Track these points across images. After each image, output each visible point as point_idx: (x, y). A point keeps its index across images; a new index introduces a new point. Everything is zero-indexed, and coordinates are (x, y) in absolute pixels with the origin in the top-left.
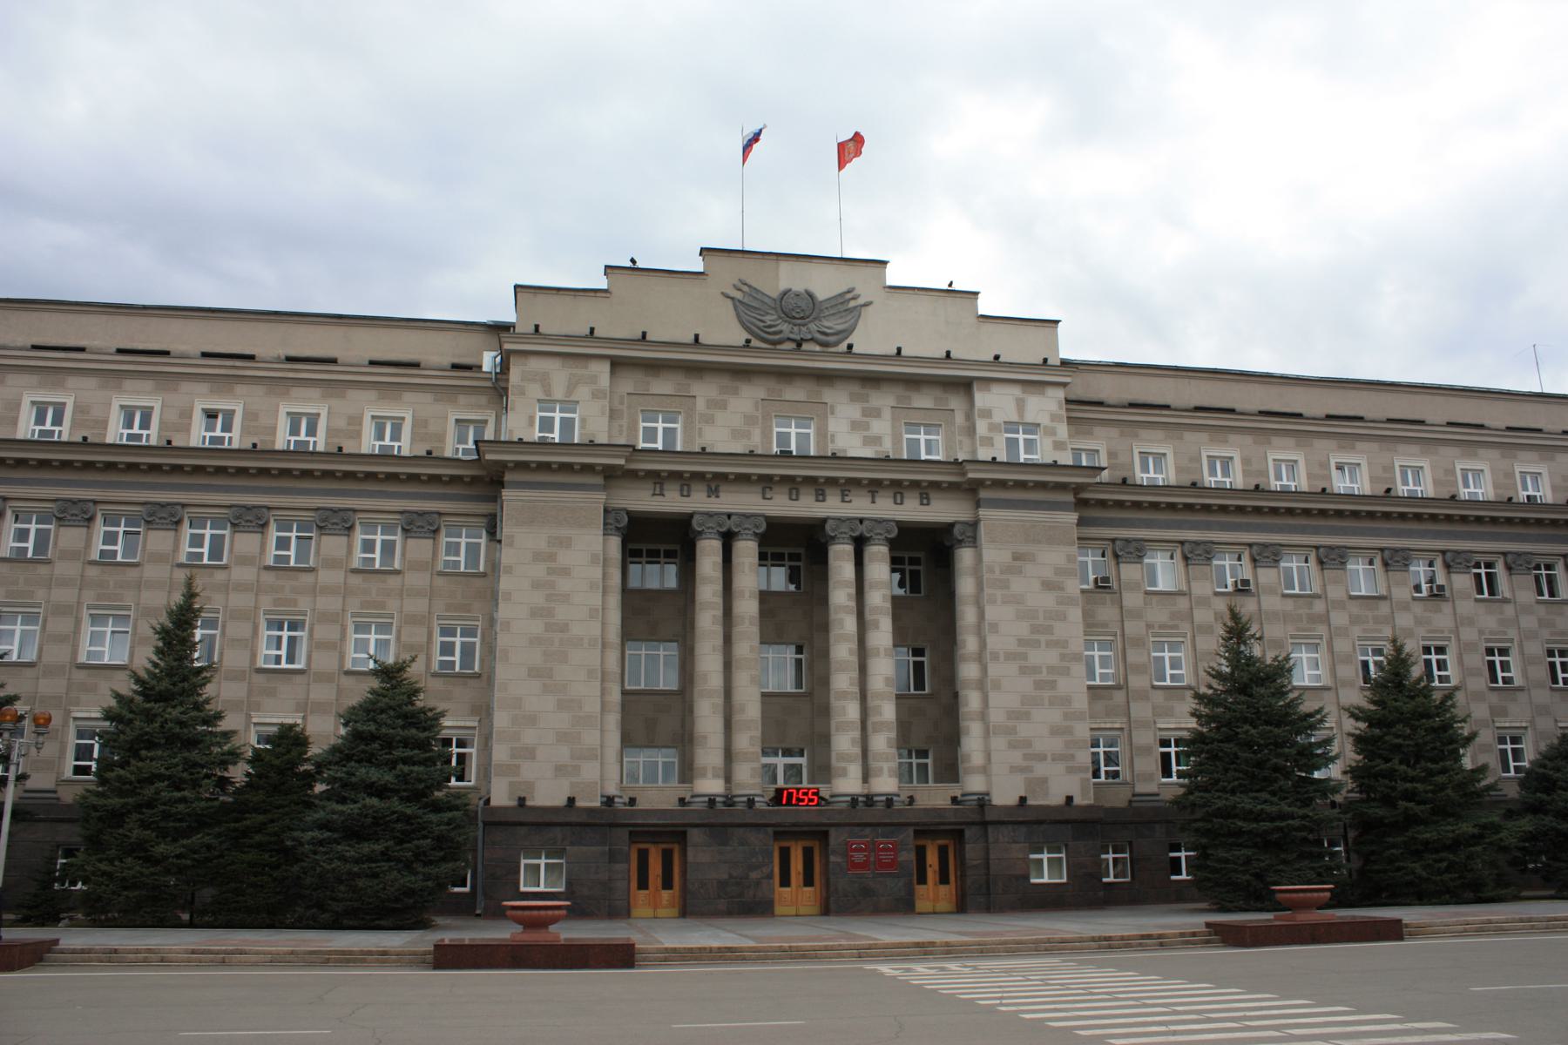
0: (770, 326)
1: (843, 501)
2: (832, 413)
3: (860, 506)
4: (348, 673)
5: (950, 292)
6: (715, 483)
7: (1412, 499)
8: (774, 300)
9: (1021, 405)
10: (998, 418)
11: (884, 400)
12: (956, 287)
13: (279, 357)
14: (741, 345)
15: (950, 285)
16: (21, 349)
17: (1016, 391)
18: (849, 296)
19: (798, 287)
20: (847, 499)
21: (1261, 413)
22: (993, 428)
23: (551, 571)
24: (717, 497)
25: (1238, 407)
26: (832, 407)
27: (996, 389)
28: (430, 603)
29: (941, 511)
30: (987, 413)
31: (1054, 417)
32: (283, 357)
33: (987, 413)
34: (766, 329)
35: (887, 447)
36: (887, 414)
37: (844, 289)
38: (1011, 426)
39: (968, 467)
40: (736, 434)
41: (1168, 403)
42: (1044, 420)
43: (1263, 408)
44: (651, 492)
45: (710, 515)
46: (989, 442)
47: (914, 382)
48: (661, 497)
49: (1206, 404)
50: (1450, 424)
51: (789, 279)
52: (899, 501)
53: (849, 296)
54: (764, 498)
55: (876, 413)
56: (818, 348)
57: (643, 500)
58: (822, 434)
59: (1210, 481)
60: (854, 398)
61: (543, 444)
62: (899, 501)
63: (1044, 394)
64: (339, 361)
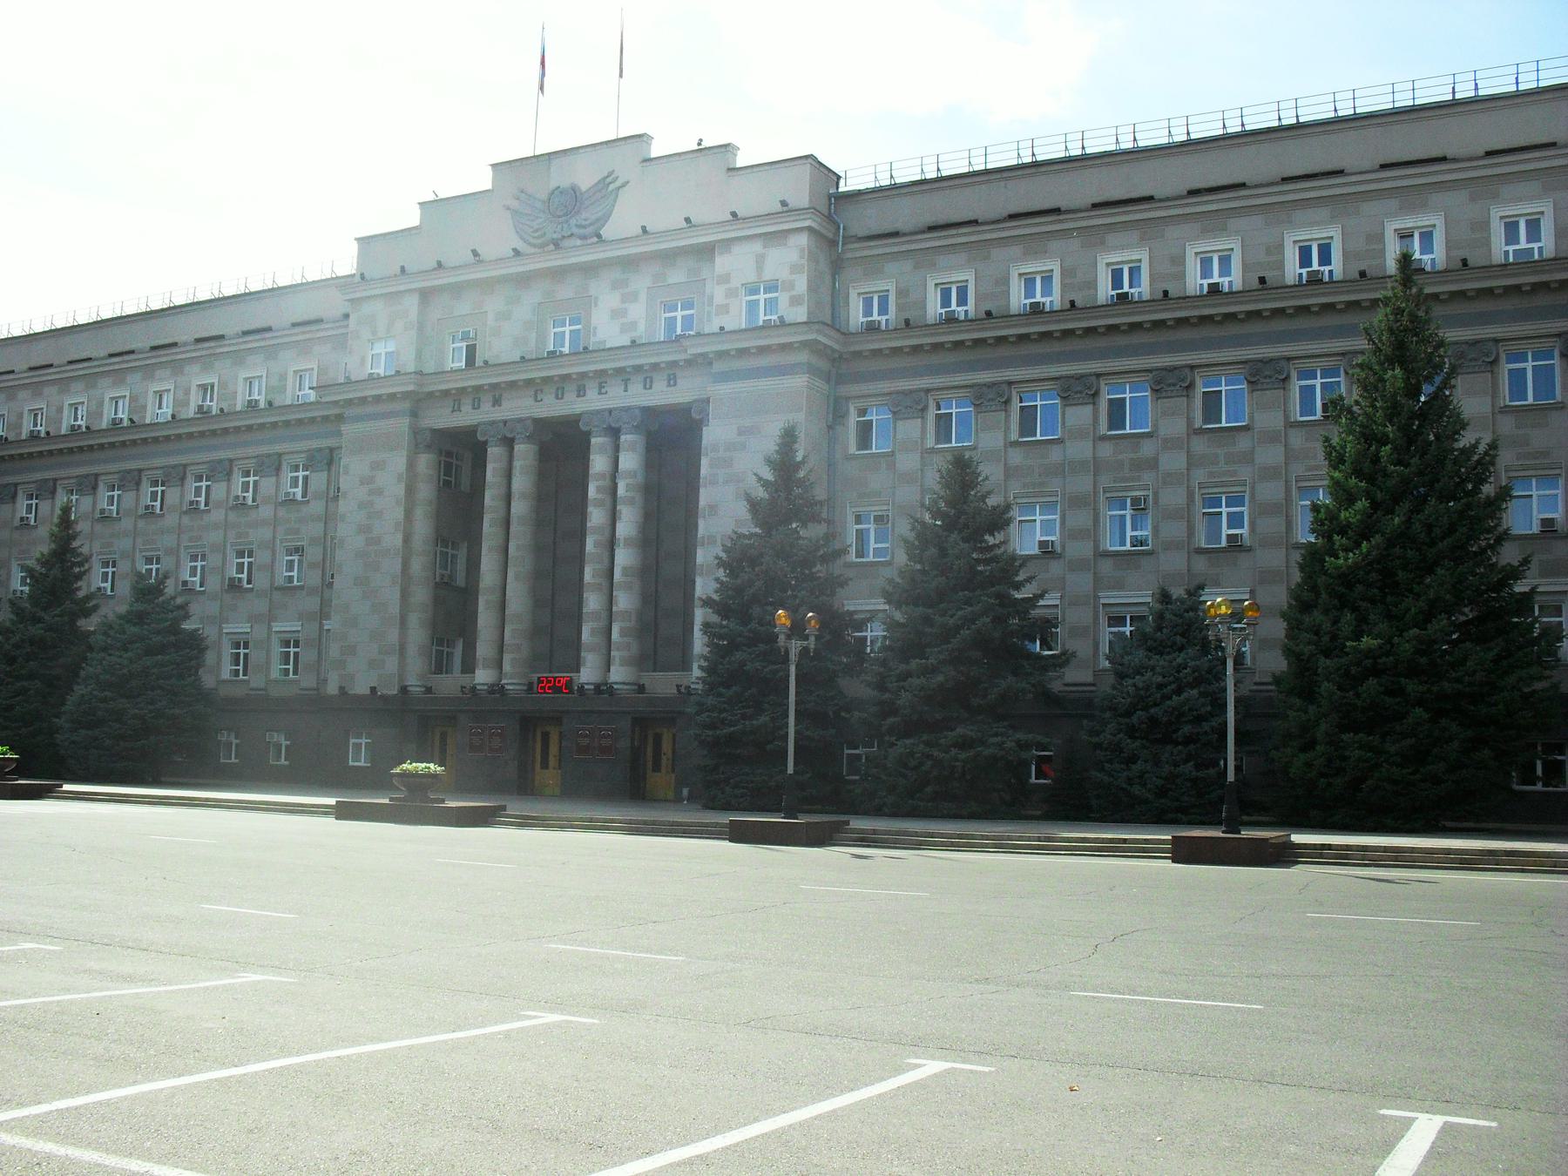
0: (537, 231)
1: (600, 393)
2: (596, 305)
3: (618, 397)
5: (701, 151)
7: (1525, 263)
8: (544, 202)
9: (760, 260)
10: (736, 282)
11: (641, 282)
12: (705, 144)
13: (238, 334)
14: (511, 256)
15: (699, 144)
16: (102, 359)
17: (757, 247)
18: (609, 180)
19: (565, 183)
20: (603, 391)
22: (732, 293)
23: (371, 492)
24: (500, 406)
25: (1063, 205)
26: (596, 298)
27: (737, 249)
28: (325, 527)
31: (795, 269)
32: (240, 333)
33: (725, 279)
34: (533, 234)
35: (641, 333)
36: (643, 297)
41: (1240, 180)
42: (784, 274)
44: (451, 409)
45: (493, 423)
46: (724, 309)
47: (669, 257)
48: (458, 413)
50: (1384, 167)
51: (559, 177)
52: (648, 386)
53: (609, 180)
54: (536, 401)
55: (631, 297)
56: (579, 242)
57: (443, 418)
59: (1507, 253)
60: (615, 285)
61: (372, 378)
62: (648, 386)
63: (785, 245)
64: (273, 329)
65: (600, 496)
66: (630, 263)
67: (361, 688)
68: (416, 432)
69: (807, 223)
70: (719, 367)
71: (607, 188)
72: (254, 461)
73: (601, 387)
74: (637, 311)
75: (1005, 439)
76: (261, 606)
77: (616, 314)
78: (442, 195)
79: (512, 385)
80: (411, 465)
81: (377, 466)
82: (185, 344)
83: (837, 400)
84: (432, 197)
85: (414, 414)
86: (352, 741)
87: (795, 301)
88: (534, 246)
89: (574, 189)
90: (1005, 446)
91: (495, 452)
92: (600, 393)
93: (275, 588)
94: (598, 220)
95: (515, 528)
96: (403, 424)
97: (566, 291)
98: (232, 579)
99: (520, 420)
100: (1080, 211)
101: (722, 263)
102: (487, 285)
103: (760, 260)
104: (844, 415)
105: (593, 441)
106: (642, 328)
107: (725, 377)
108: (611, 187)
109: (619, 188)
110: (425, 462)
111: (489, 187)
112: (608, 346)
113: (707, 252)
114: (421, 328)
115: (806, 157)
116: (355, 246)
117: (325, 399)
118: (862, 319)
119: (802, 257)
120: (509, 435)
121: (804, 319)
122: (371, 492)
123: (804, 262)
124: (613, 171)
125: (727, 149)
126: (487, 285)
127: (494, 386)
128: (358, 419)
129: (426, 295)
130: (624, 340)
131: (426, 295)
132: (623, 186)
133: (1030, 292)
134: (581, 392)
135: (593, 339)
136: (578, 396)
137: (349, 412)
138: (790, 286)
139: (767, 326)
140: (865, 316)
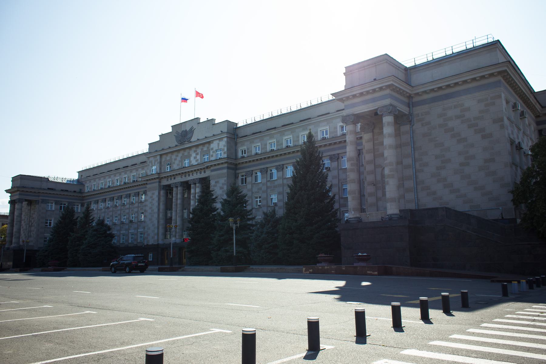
0: (179, 140)
1: (192, 175)
4: (139, 222)
6: (174, 176)
9: (218, 144)
10: (214, 150)
19: (185, 130)
21: (283, 126)
22: (213, 152)
29: (207, 173)
30: (212, 149)
31: (224, 146)
33: (212, 149)
36: (199, 154)
37: (191, 127)
38: (217, 151)
39: (204, 164)
40: (178, 165)
42: (222, 147)
43: (283, 125)
49: (270, 128)
51: (183, 129)
55: (197, 154)
56: (187, 142)
57: (165, 182)
58: (190, 162)
61: (152, 174)
65: (193, 198)
66: (197, 146)
67: (150, 243)
68: (160, 186)
69: (226, 136)
70: (212, 168)
71: (192, 131)
72: (134, 194)
73: (192, 174)
74: (198, 157)
75: (267, 180)
76: (127, 227)
77: (195, 158)
78: (163, 134)
79: (176, 175)
80: (159, 193)
81: (153, 194)
82: (121, 168)
83: (236, 174)
84: (161, 134)
85: (160, 182)
86: (149, 255)
87: (224, 153)
88: (179, 144)
89: (186, 130)
90: (267, 182)
91: (174, 189)
92: (192, 175)
93: (138, 222)
94: (190, 137)
95: (178, 206)
96: (157, 185)
97: (186, 154)
98: (130, 220)
99: (178, 182)
100: (280, 127)
101: (212, 146)
102: (172, 152)
103: (218, 144)
104: (238, 177)
105: (192, 186)
106: (199, 160)
107: (212, 171)
108: (192, 130)
109: (194, 130)
110: (162, 192)
111: (171, 131)
112: (194, 165)
113: (209, 143)
114: (160, 163)
115: (226, 121)
116: (148, 145)
117: (142, 180)
118: (241, 155)
119: (226, 143)
120: (177, 186)
121: (226, 157)
122: (152, 200)
123: (226, 144)
124: (192, 127)
125: (213, 120)
126: (172, 152)
127: (173, 175)
128: (150, 184)
129: (161, 155)
130: (196, 163)
131: (161, 155)
132: (195, 129)
133: (271, 147)
134: (189, 175)
135: (191, 164)
136: (189, 176)
137: (148, 182)
138: (223, 150)
139: (220, 159)
140: (242, 155)
